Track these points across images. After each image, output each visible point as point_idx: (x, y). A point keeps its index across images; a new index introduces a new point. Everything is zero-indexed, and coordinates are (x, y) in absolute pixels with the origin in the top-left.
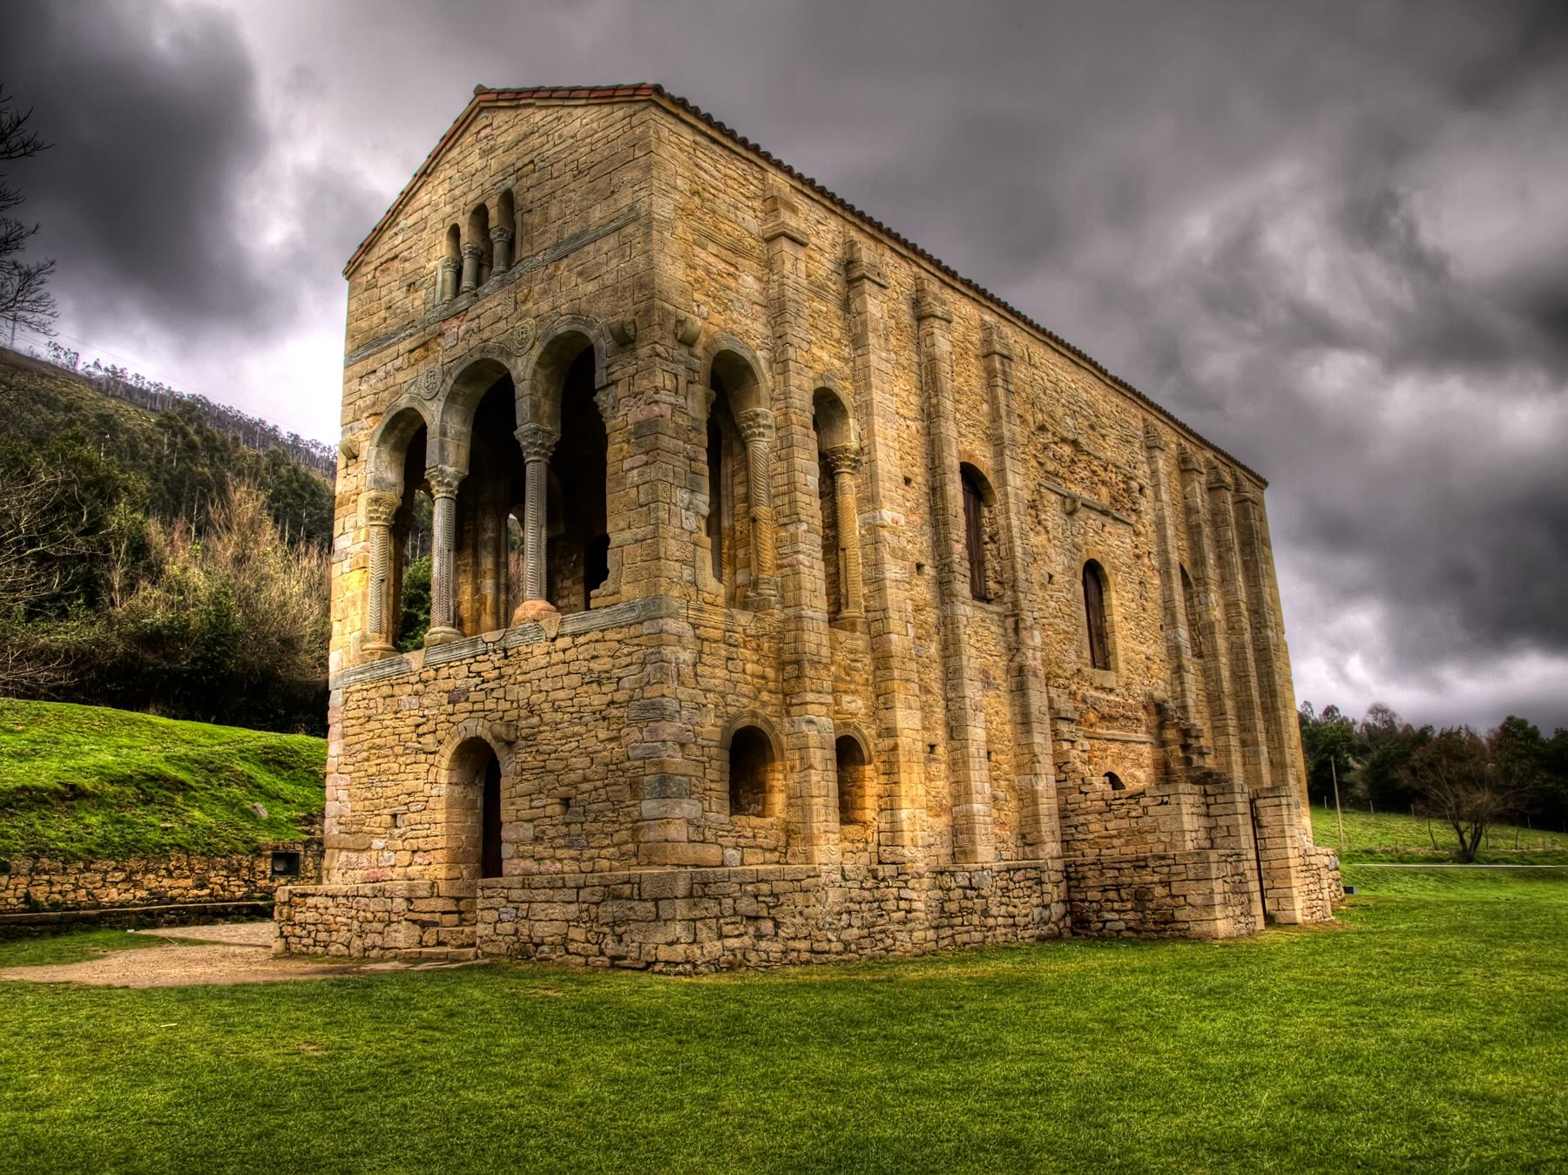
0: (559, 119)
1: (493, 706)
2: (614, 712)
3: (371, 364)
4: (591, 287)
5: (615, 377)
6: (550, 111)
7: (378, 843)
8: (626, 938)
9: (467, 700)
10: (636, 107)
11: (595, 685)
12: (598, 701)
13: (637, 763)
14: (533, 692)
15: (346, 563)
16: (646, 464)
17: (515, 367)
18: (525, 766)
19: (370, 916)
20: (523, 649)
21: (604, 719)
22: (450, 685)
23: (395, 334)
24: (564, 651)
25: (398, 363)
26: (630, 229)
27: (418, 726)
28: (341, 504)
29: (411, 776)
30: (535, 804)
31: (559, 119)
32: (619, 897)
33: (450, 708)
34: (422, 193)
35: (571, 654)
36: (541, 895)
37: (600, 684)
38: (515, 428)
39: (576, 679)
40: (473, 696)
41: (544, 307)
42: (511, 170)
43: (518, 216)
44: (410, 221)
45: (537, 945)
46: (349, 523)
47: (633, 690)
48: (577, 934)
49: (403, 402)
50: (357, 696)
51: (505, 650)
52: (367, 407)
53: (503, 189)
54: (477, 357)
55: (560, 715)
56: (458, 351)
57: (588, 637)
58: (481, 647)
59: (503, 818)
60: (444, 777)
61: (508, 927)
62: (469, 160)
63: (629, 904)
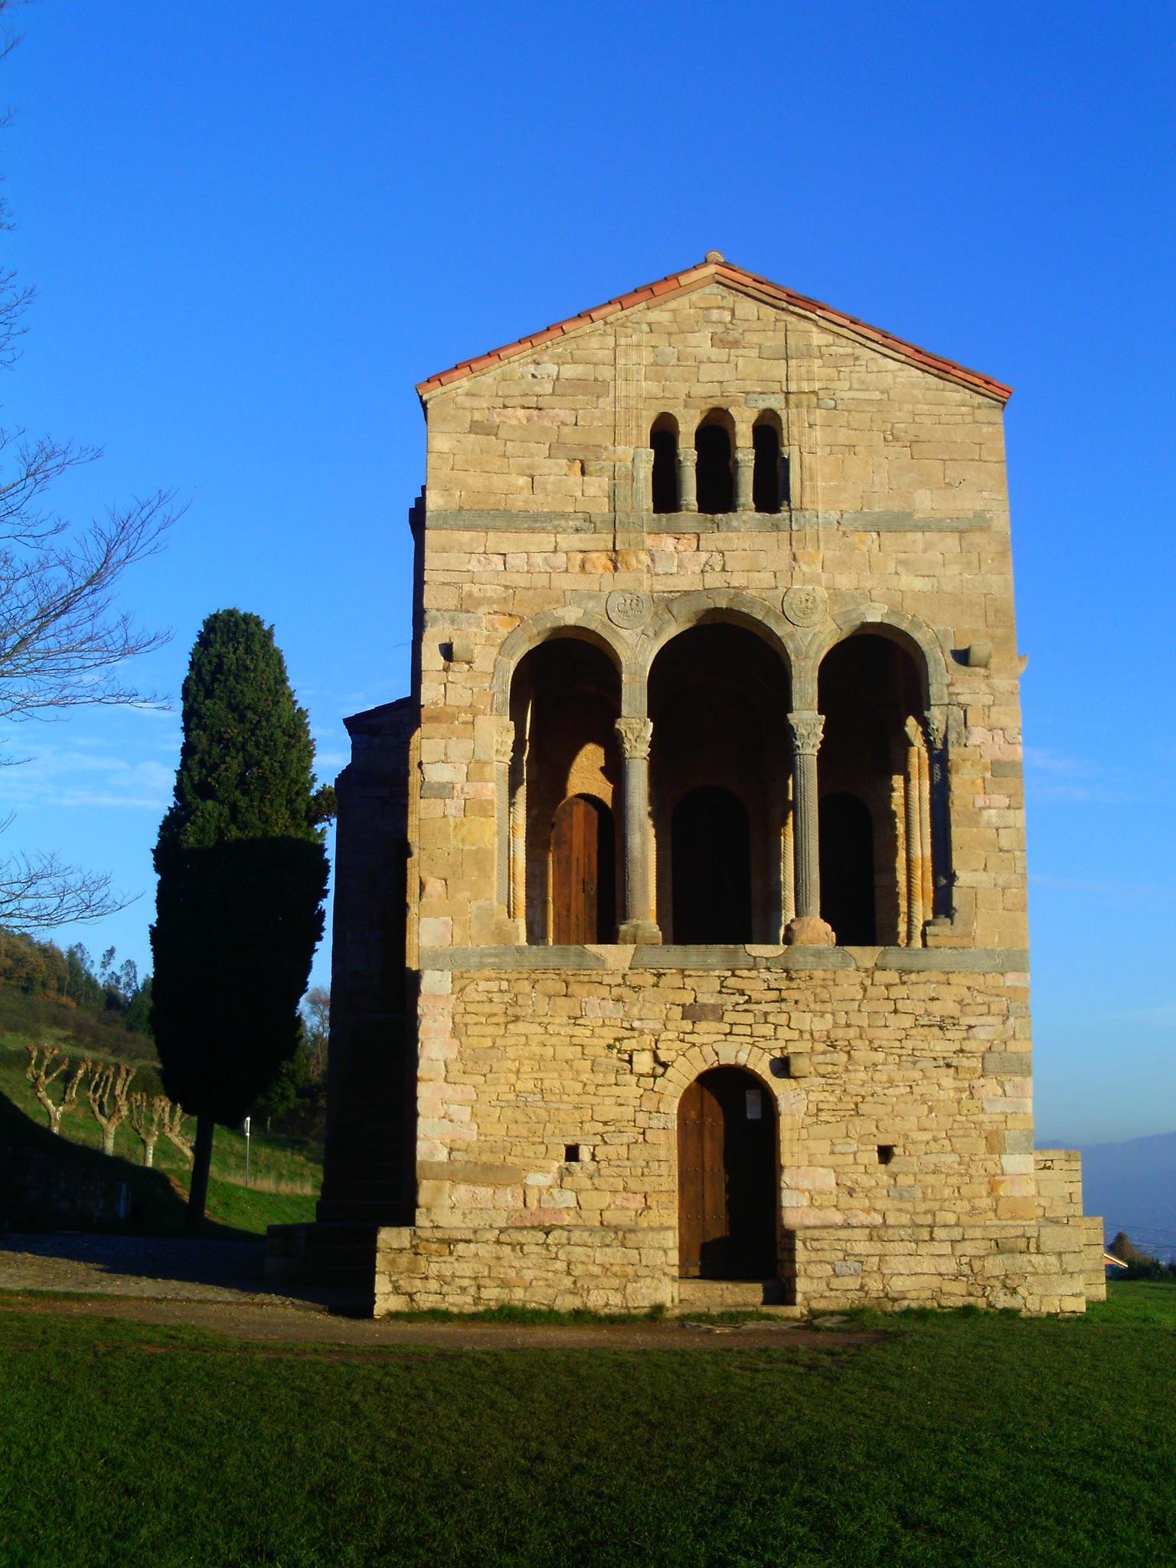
0: (857, 359)
1: (768, 1030)
2: (965, 1062)
3: (494, 541)
4: (919, 584)
5: (962, 699)
6: (844, 341)
7: (536, 1179)
8: (1020, 1290)
9: (721, 1019)
10: (980, 399)
11: (936, 1030)
12: (941, 1047)
13: (996, 1117)
14: (836, 1025)
15: (453, 807)
16: (1009, 808)
17: (792, 636)
18: (821, 1106)
19: (596, 1270)
20: (819, 974)
21: (948, 1066)
22: (689, 999)
23: (549, 516)
24: (888, 986)
25: (560, 559)
26: (976, 538)
27: (616, 1039)
28: (435, 719)
29: (608, 1101)
30: (837, 1149)
31: (857, 359)
32: (1011, 1251)
33: (687, 1026)
34: (594, 342)
35: (895, 992)
36: (900, 1248)
37: (941, 1028)
38: (790, 710)
39: (907, 1021)
40: (729, 1017)
41: (845, 581)
42: (776, 387)
43: (791, 451)
44: (569, 371)
45: (895, 1300)
46: (460, 748)
47: (991, 1041)
48: (958, 1288)
49: (571, 616)
50: (483, 985)
51: (787, 971)
52: (489, 601)
53: (763, 405)
54: (723, 604)
55: (880, 1056)
56: (684, 583)
57: (923, 977)
58: (742, 960)
59: (785, 1159)
60: (672, 1107)
61: (853, 1283)
62: (692, 339)
63: (1025, 1258)
